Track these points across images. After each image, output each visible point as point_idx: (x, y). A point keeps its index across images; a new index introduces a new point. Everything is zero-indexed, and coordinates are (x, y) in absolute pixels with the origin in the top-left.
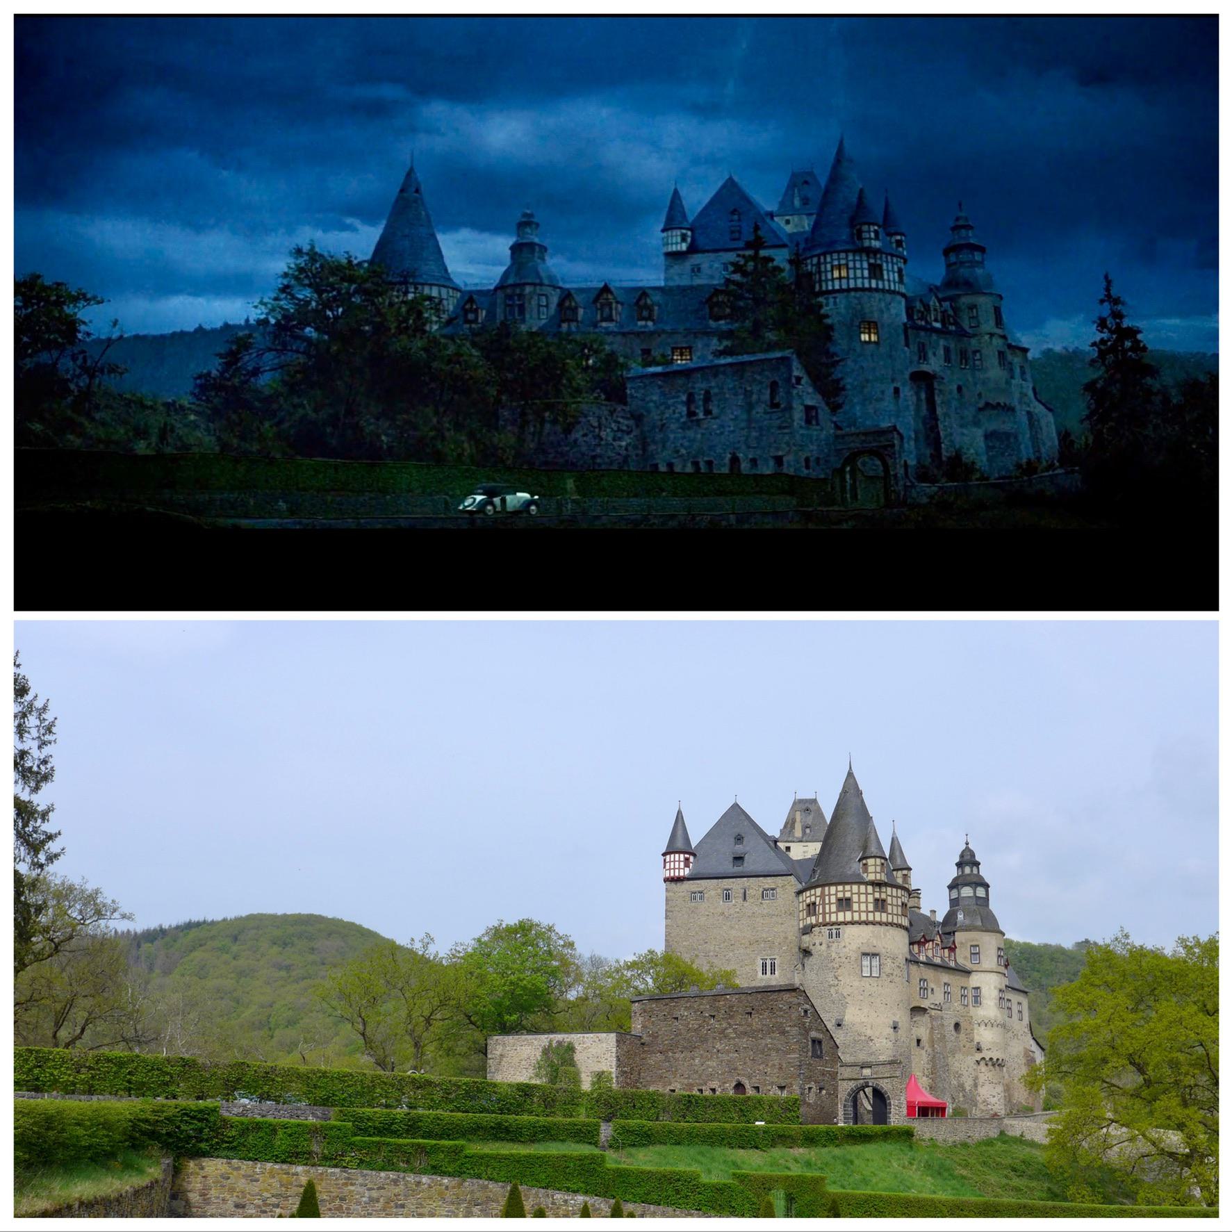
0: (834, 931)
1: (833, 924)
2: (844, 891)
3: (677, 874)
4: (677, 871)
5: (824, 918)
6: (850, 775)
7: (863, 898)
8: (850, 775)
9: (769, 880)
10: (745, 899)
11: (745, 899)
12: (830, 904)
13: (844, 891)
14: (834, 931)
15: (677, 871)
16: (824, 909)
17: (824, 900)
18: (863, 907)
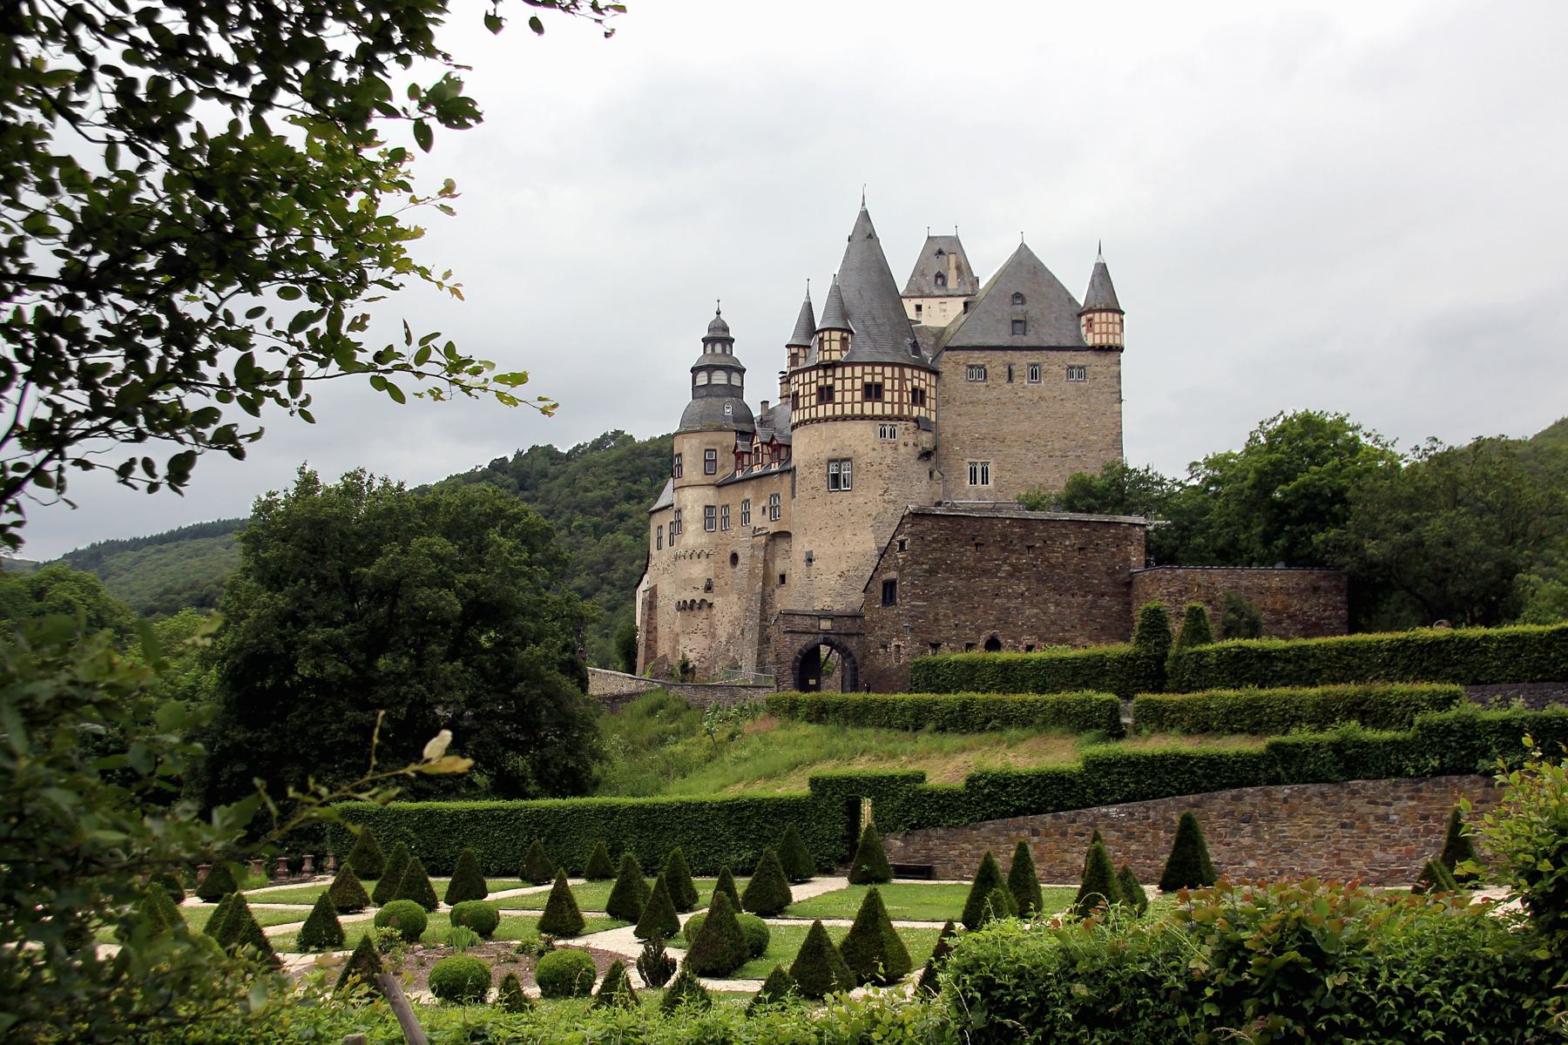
0: (888, 429)
1: (889, 418)
2: (873, 374)
3: (1104, 341)
4: (1104, 336)
5: (901, 409)
6: (865, 216)
7: (848, 384)
8: (865, 216)
9: (976, 354)
10: (1010, 379)
11: (1010, 379)
12: (893, 390)
13: (873, 374)
14: (888, 429)
15: (1104, 336)
16: (901, 397)
17: (900, 385)
18: (848, 397)
